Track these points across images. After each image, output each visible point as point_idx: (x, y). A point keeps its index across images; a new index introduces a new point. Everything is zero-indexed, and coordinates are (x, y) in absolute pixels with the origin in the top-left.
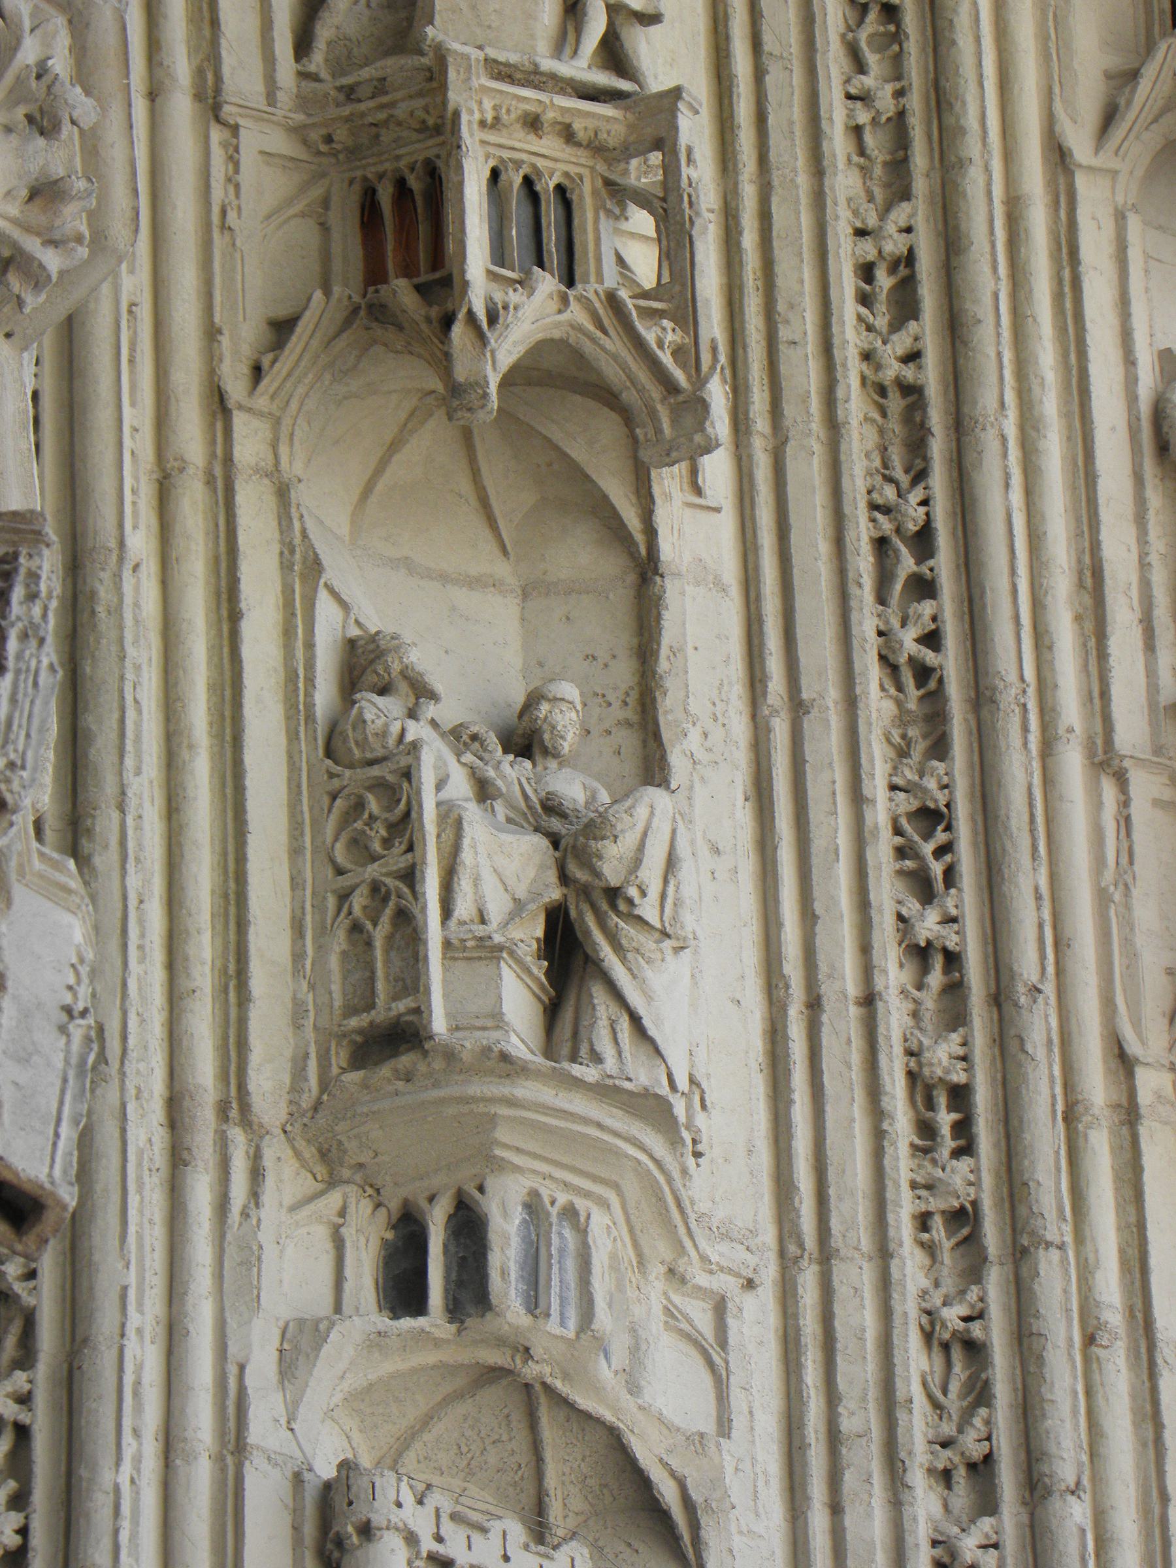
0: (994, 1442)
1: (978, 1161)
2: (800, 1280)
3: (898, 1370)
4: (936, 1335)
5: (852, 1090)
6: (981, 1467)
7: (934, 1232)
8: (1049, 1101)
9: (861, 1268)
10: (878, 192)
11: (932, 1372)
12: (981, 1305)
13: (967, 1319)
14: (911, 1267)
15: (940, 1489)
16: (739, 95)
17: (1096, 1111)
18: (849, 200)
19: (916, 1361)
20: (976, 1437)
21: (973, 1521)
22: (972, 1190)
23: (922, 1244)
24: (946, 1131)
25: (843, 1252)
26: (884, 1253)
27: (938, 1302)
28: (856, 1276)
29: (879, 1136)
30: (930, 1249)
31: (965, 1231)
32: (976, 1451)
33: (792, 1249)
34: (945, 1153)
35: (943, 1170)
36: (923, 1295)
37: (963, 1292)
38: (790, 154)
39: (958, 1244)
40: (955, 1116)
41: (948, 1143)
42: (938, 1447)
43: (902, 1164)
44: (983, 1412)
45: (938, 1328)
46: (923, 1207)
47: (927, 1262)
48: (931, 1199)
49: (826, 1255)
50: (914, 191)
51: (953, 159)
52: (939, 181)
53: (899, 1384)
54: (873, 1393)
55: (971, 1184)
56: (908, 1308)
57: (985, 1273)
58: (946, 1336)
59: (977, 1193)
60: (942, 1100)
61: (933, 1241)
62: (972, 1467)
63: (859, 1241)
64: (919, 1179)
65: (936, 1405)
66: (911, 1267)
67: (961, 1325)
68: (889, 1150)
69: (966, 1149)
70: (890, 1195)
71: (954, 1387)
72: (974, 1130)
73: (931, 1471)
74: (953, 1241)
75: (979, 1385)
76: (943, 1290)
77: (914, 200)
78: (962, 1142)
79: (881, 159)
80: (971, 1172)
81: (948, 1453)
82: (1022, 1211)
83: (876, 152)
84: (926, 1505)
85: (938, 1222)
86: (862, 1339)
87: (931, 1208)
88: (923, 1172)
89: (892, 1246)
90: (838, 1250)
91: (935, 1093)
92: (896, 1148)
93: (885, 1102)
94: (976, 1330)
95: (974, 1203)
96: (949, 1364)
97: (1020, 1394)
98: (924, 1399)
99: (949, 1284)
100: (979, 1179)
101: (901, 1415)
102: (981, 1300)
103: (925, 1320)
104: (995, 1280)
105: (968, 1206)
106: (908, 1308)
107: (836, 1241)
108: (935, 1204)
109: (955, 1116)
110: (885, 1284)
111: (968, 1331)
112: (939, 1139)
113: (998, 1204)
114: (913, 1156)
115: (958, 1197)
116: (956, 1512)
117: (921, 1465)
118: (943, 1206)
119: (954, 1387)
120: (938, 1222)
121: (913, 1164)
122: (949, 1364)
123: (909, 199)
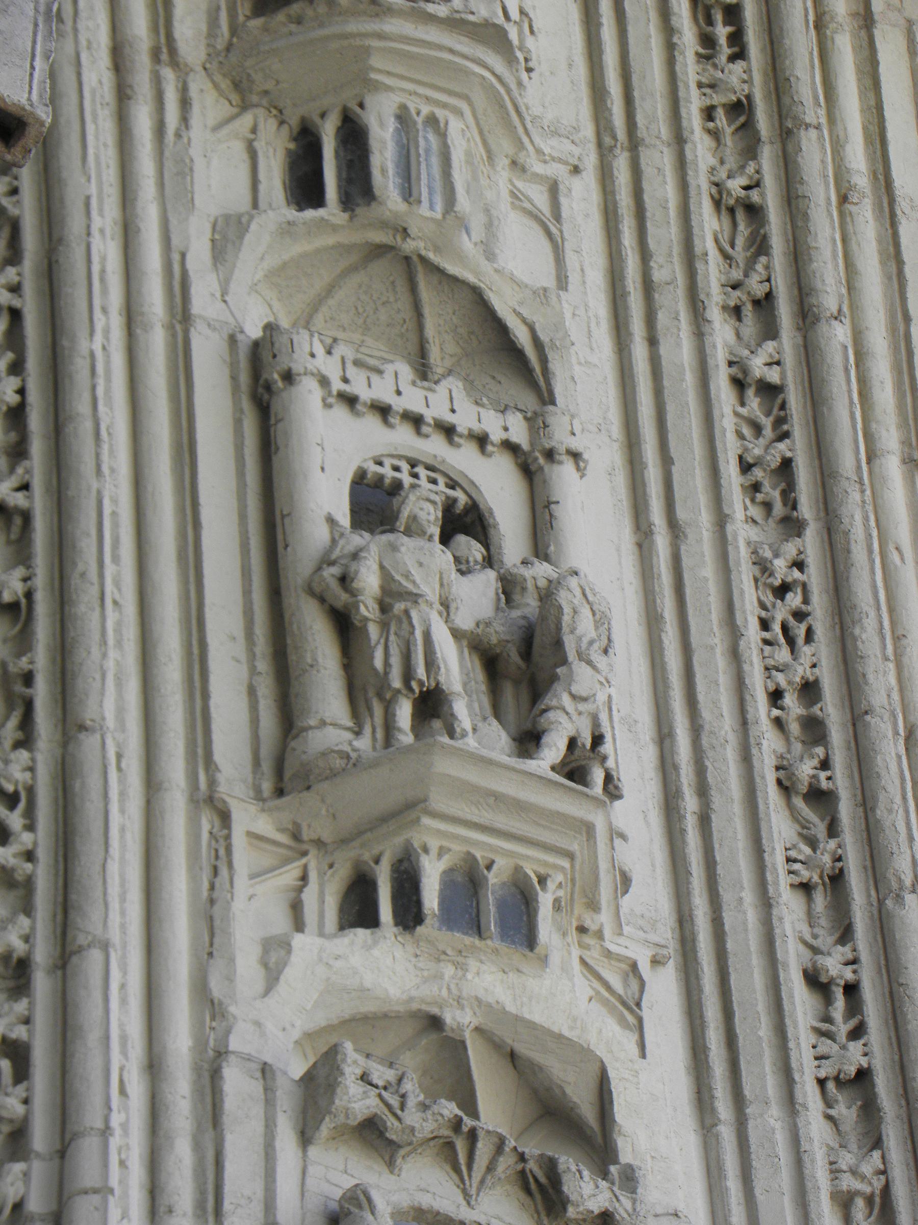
0: (773, 282)
1: (749, 63)
2: (615, 165)
3: (696, 231)
4: (724, 201)
5: (647, 13)
6: (764, 303)
7: (718, 122)
8: (803, 13)
9: (662, 152)
11: (722, 231)
12: (757, 176)
13: (747, 188)
14: (701, 149)
15: (733, 321)
17: (840, 19)
19: (709, 223)
20: (759, 279)
21: (759, 345)
22: (746, 86)
23: (709, 131)
24: (723, 41)
25: (647, 141)
26: (679, 140)
27: (724, 175)
28: (658, 160)
29: (670, 49)
30: (715, 135)
31: (742, 119)
32: (759, 290)
33: (608, 140)
34: (723, 58)
35: (722, 72)
36: (712, 170)
37: (743, 167)
39: (737, 130)
40: (729, 29)
41: (725, 50)
42: (730, 289)
43: (690, 69)
44: (763, 259)
45: (724, 196)
46: (708, 102)
47: (713, 144)
48: (714, 96)
49: (634, 144)
53: (697, 241)
54: (677, 250)
55: (745, 82)
56: (701, 182)
57: (759, 151)
58: (732, 202)
59: (750, 89)
60: (718, 17)
61: (717, 128)
62: (756, 303)
63: (660, 132)
64: (704, 80)
65: (726, 257)
66: (701, 149)
67: (743, 193)
68: (679, 58)
69: (740, 55)
70: (682, 94)
71: (740, 242)
72: (745, 39)
73: (725, 308)
74: (733, 127)
75: (759, 239)
76: (727, 166)
78: (736, 49)
80: (745, 72)
81: (737, 293)
82: (786, 100)
84: (722, 334)
85: (720, 113)
86: (666, 208)
87: (715, 103)
88: (706, 74)
89: (686, 134)
90: (643, 140)
91: (713, 12)
92: (685, 57)
93: (675, 22)
94: (755, 196)
95: (748, 97)
96: (735, 224)
97: (791, 244)
98: (717, 253)
99: (732, 162)
100: (751, 77)
101: (700, 266)
102: (758, 172)
103: (714, 190)
104: (767, 156)
105: (743, 99)
106: (701, 182)
107: (642, 132)
108: (717, 99)
109: (729, 29)
110: (682, 164)
111: (748, 197)
112: (718, 48)
113: (767, 97)
114: (698, 62)
115: (735, 93)
116: (746, 338)
117: (717, 304)
118: (724, 100)
119: (740, 242)
120: (720, 113)
121: (699, 68)
122: (735, 224)
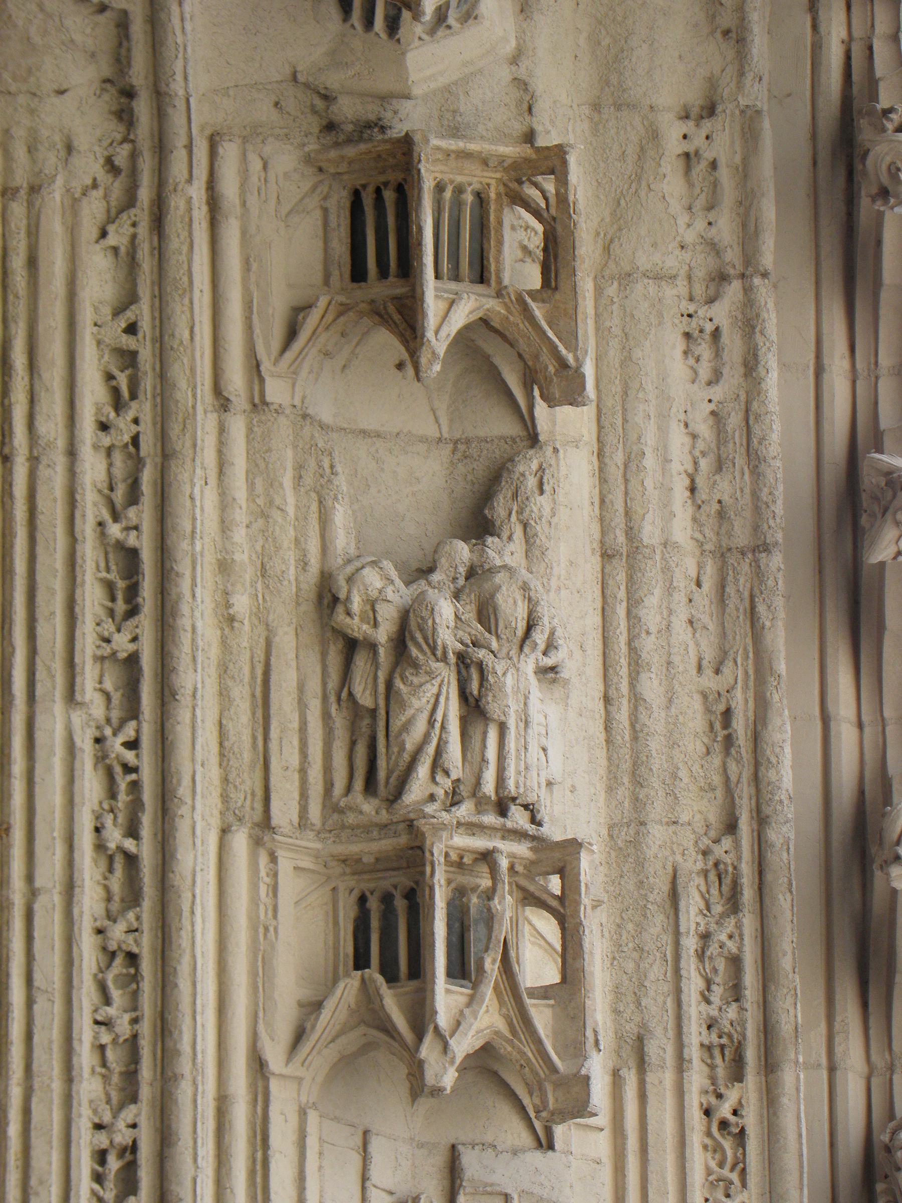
10: (115, 1096)
16: (13, 1019)
18: (91, 1102)
38: (49, 1065)
50: (140, 1097)
51: (170, 1074)
52: (159, 1089)
77: (139, 1104)
79: (117, 1070)
83: (114, 1065)
123: (136, 1103)
